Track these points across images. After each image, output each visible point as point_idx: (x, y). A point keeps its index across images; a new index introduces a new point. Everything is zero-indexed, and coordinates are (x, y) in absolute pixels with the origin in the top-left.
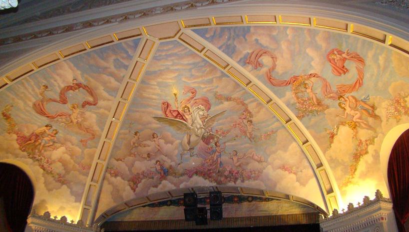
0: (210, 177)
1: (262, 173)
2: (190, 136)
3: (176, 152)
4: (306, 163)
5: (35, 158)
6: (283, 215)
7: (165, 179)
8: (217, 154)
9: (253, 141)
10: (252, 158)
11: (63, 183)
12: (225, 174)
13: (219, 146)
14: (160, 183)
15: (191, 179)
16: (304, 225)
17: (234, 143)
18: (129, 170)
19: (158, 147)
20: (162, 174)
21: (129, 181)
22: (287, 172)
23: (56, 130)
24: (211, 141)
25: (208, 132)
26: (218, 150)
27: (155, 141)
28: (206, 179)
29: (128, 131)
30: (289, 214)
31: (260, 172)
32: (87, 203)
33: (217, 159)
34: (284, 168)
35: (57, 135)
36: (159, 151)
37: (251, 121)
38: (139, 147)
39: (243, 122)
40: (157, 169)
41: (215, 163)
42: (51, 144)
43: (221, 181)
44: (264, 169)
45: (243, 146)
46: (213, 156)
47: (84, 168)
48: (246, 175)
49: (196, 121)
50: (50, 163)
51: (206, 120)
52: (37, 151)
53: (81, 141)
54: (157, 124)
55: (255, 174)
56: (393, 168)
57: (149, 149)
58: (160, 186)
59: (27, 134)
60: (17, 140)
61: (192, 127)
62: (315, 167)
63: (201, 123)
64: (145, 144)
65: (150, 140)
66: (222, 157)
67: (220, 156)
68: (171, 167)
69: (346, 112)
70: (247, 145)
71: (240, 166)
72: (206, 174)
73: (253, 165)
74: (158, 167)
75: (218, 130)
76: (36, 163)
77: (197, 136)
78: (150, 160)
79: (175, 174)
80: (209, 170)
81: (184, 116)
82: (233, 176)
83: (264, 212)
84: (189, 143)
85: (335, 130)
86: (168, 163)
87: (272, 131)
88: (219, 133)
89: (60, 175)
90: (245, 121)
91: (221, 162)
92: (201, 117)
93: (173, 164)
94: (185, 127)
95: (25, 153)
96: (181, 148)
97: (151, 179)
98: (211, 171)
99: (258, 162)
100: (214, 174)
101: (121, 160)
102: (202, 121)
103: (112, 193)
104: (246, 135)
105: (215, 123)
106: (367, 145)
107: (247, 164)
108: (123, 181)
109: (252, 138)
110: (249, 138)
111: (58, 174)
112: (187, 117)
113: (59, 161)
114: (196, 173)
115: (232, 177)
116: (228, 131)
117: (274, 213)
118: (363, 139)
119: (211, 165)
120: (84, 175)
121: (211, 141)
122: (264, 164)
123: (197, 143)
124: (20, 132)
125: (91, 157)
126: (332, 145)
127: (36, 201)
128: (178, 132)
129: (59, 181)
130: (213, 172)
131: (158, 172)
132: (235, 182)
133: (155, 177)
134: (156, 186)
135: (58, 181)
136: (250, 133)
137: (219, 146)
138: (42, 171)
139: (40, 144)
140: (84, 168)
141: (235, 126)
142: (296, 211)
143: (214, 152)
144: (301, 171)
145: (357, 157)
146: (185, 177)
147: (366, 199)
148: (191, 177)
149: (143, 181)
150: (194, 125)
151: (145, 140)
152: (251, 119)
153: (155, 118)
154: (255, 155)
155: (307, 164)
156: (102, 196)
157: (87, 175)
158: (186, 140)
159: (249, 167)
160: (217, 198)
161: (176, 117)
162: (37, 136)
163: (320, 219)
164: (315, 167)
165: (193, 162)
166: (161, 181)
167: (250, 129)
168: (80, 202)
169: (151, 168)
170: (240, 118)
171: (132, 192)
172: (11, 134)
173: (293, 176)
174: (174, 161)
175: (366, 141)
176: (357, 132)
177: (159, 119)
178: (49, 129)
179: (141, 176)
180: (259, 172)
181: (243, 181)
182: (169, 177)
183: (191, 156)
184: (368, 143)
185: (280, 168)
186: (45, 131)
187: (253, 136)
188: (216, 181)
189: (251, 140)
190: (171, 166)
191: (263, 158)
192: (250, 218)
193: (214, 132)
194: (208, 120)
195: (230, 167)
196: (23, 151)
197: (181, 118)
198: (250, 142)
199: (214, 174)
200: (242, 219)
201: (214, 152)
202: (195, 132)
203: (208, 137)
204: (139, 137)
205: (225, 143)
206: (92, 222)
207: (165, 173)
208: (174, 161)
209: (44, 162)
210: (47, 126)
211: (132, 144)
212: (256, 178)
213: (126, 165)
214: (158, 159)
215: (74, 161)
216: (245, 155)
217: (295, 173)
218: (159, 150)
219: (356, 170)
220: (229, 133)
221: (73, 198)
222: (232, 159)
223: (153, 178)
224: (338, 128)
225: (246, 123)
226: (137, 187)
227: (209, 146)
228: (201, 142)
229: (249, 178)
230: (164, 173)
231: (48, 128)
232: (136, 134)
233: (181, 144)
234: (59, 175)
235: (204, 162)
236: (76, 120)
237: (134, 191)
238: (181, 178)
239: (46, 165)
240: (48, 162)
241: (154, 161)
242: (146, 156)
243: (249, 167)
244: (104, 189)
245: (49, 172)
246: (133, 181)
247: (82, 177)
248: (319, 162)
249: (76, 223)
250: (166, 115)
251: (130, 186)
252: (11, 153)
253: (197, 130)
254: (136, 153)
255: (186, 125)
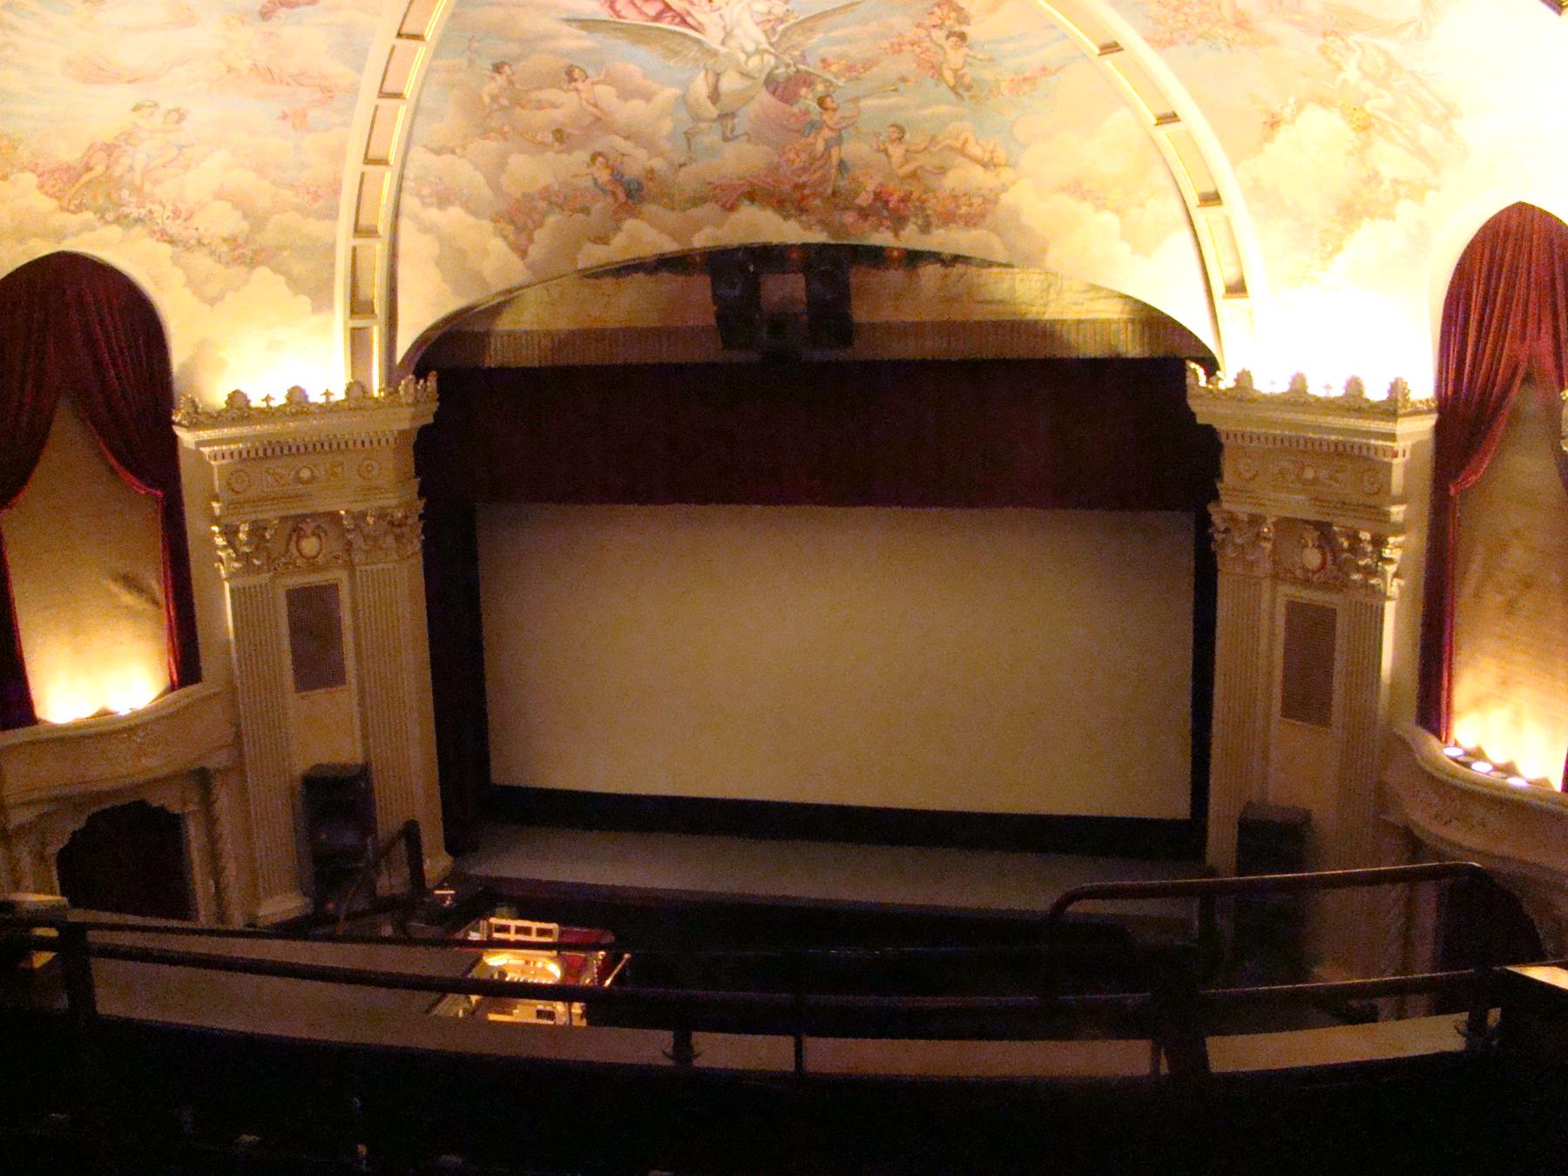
0: (803, 211)
1: (996, 201)
2: (718, 76)
3: (667, 126)
4: (1160, 178)
5: (126, 216)
6: (1063, 322)
7: (635, 215)
8: (826, 133)
9: (966, 95)
10: (962, 152)
11: (252, 263)
12: (858, 201)
13: (835, 110)
14: (619, 229)
15: (734, 217)
16: (1133, 361)
17: (893, 100)
18: (489, 183)
19: (591, 108)
20: (622, 197)
21: (495, 221)
22: (1087, 207)
23: (177, 110)
24: (803, 91)
25: (788, 66)
26: (830, 123)
27: (576, 90)
28: (786, 217)
29: (465, 62)
30: (1083, 317)
31: (990, 200)
32: (358, 306)
33: (828, 148)
34: (1077, 188)
35: (184, 124)
36: (600, 122)
37: (962, 37)
38: (518, 110)
39: (929, 35)
40: (600, 181)
41: (819, 163)
42: (172, 153)
43: (843, 225)
44: (1005, 188)
45: (926, 112)
46: (811, 140)
47: (316, 197)
48: (939, 209)
49: (737, 32)
50: (184, 215)
51: (780, 28)
52: (125, 193)
53: (285, 117)
54: (579, 38)
55: (971, 205)
56: (1469, 295)
57: (558, 115)
58: (619, 240)
59: (68, 153)
60: (41, 187)
61: (723, 50)
62: (1193, 201)
63: (762, 38)
64: (539, 101)
65: (561, 88)
66: (845, 147)
67: (839, 140)
68: (651, 174)
69: (1341, 76)
70: (943, 109)
71: (913, 175)
72: (789, 202)
73: (964, 177)
74: (604, 176)
75: (830, 59)
76: (138, 229)
77: (744, 75)
78: (569, 151)
79: (671, 197)
80: (797, 187)
81: (689, 13)
82: (889, 209)
83: (994, 307)
84: (715, 96)
85: (1288, 111)
86: (638, 161)
87: (1044, 69)
88: (834, 68)
89: (235, 239)
90: (939, 35)
91: (841, 163)
92: (761, 19)
93: (658, 164)
94: (696, 48)
95: (88, 215)
96: (684, 115)
97: (581, 216)
98: (806, 192)
99: (985, 165)
100: (818, 202)
101: (453, 152)
102: (765, 32)
103: (439, 263)
104: (941, 74)
105: (816, 39)
106: (1396, 195)
107: (942, 171)
108: (471, 220)
109: (961, 88)
110: (953, 89)
111: (225, 240)
112: (701, 18)
113: (219, 196)
114: (752, 196)
115: (885, 213)
116: (869, 64)
117: (1033, 313)
118: (1387, 172)
119: (804, 169)
120: (321, 216)
121: (803, 91)
122: (1006, 174)
123: (745, 98)
124: (41, 161)
125: (338, 156)
126: (1267, 147)
127: (179, 356)
128: (672, 63)
129: (239, 260)
130: (815, 195)
131: (604, 192)
132: (896, 235)
133: (597, 208)
134: (602, 240)
135: (235, 260)
136: (955, 71)
137: (835, 110)
138: (166, 249)
139: (131, 168)
140: (316, 197)
141: (897, 49)
142: (1111, 311)
143: (816, 127)
144: (1141, 205)
145: (1350, 212)
146: (711, 209)
147: (1355, 385)
148: (732, 208)
149: (551, 220)
150: (732, 43)
151: (540, 88)
152: (964, 28)
153: (567, 21)
154: (972, 142)
155: (1163, 181)
156: (403, 272)
157: (332, 214)
158: (701, 87)
159: (951, 181)
160: (835, 266)
161: (658, 18)
162: (110, 149)
163: (1190, 380)
164: (1193, 201)
165: (738, 159)
166: (620, 220)
167: (955, 57)
168: (330, 306)
169: (576, 176)
170: (919, 25)
171: (514, 258)
172: (12, 178)
173: (1109, 220)
174: (661, 154)
175: (1396, 181)
176: (1367, 144)
177: (587, 24)
178: (151, 114)
179: (542, 205)
180: (985, 200)
181: (925, 229)
182: (650, 208)
183: (726, 139)
184: (1402, 190)
185: (1063, 189)
186: (135, 124)
187: (967, 80)
188: (825, 224)
189: (957, 94)
190: (652, 171)
191: (1001, 155)
192: (949, 329)
193: (813, 66)
194: (787, 29)
195: (879, 179)
196: (73, 212)
197: (677, 20)
198: (952, 96)
199: (818, 202)
200: (917, 329)
201: (816, 127)
202: (738, 64)
203: (789, 79)
204: (515, 78)
205: (856, 100)
206: (391, 379)
207: (631, 194)
208: (661, 154)
209: (162, 217)
210: (136, 109)
211: (486, 99)
212: (971, 221)
213: (477, 168)
214: (598, 147)
215: (273, 183)
216: (933, 139)
217: (1117, 211)
218: (598, 119)
219: (1338, 248)
220: (875, 69)
221: (304, 302)
222: (886, 151)
223: (586, 210)
224: (1300, 107)
225: (942, 41)
226: (531, 240)
227: (795, 109)
228: (765, 97)
229: (948, 218)
230: (629, 195)
231: (146, 111)
232: (498, 68)
233: (683, 100)
234: (232, 241)
235: (776, 159)
236: (249, 62)
237: (523, 254)
238: (696, 212)
239: (174, 228)
240: (176, 214)
241: (581, 156)
242: (550, 138)
243: (951, 181)
244: (403, 247)
245: (193, 242)
246: (512, 222)
247: (314, 227)
248: (1181, 808)
249: (343, 396)
250: (617, 13)
251: (505, 238)
252: (36, 235)
253: (742, 57)
254: (506, 128)
255: (698, 42)
